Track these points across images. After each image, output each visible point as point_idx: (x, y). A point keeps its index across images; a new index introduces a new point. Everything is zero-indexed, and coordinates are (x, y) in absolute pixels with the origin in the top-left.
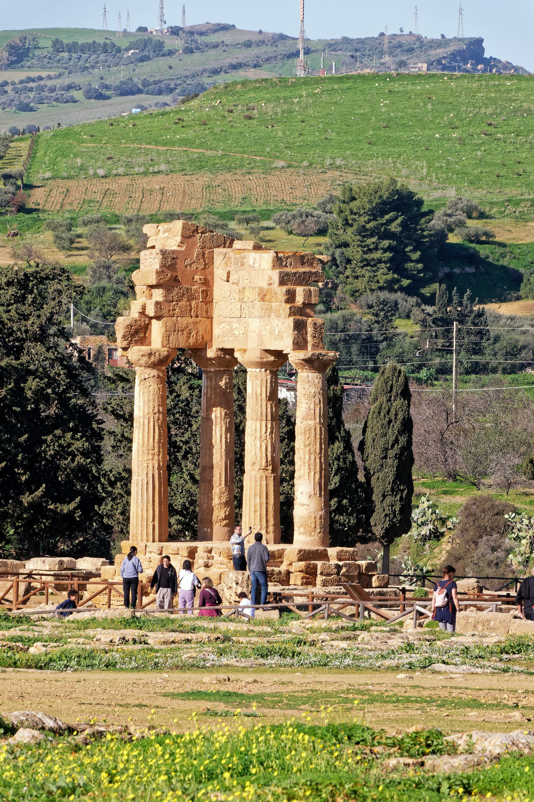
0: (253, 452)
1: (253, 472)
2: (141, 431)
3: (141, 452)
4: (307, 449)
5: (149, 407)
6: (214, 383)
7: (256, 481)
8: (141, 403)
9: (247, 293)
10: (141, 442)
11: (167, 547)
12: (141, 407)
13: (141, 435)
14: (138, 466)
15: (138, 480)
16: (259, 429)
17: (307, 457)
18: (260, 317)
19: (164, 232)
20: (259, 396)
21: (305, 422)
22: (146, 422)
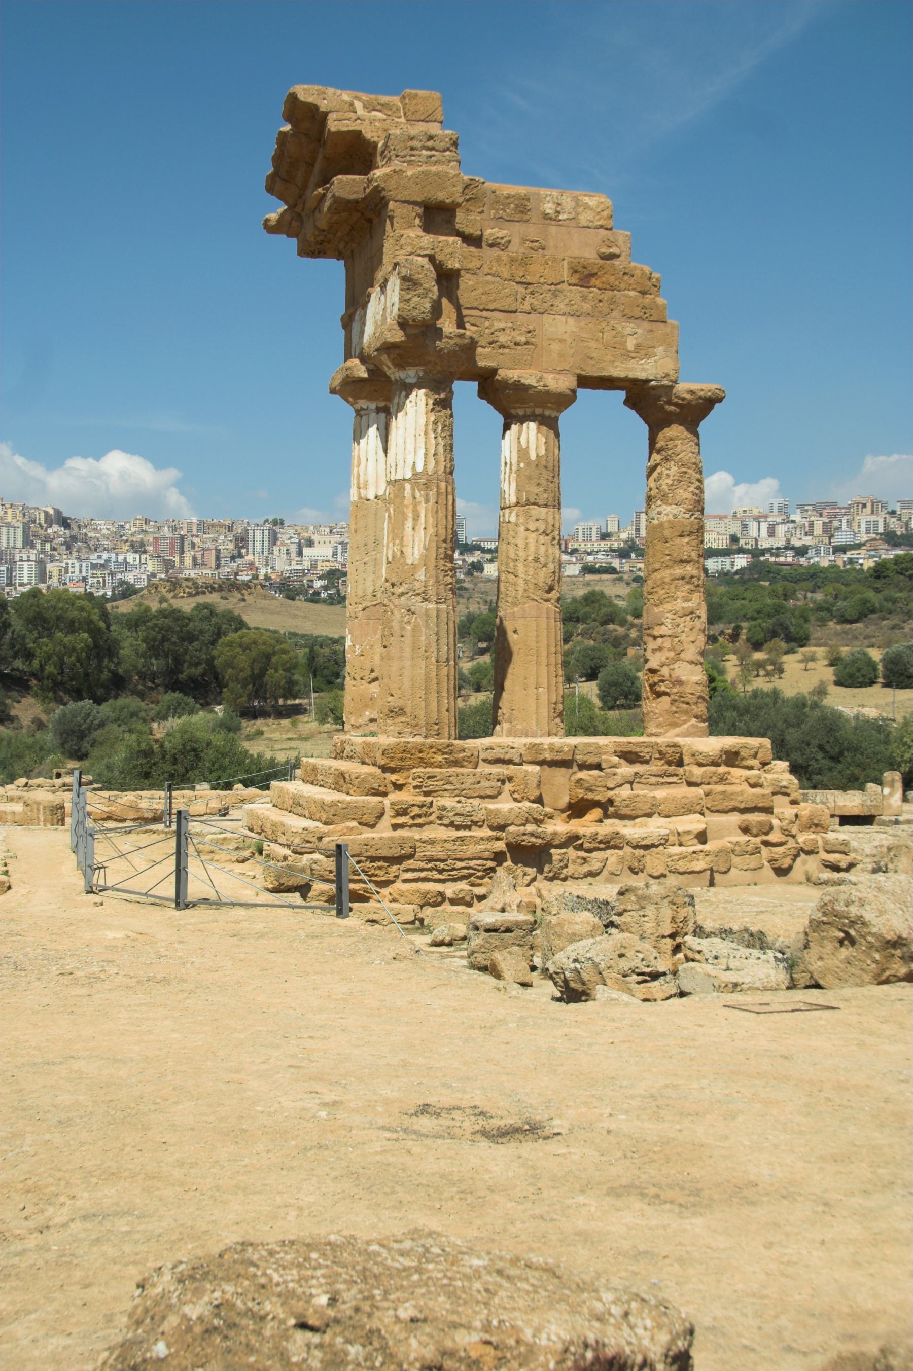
3: (442, 550)
8: (441, 449)
18: (576, 315)
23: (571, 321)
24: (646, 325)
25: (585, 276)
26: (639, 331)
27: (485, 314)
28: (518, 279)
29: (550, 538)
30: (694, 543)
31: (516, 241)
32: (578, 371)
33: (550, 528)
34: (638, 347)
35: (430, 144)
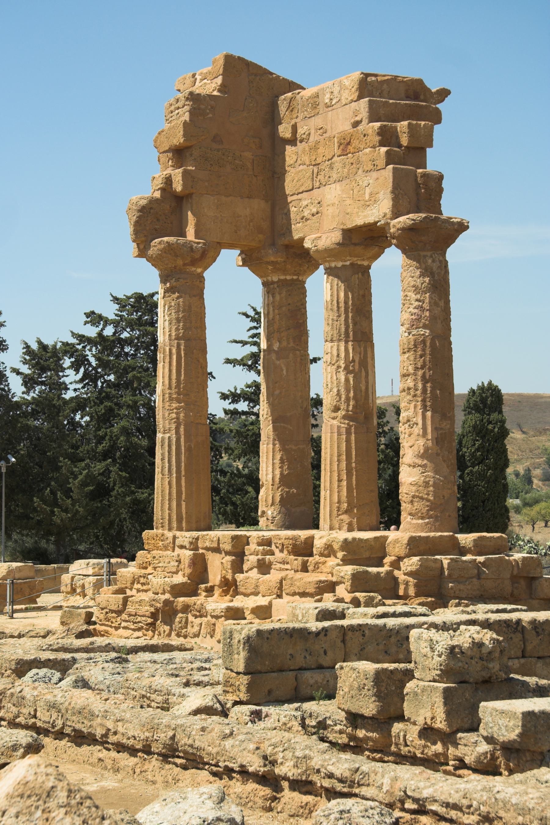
0: (335, 390)
1: (335, 422)
2: (167, 365)
4: (420, 373)
5: (177, 329)
6: (278, 297)
7: (339, 434)
8: (167, 323)
9: (321, 150)
10: (167, 382)
11: (203, 536)
12: (167, 330)
13: (167, 370)
14: (164, 418)
15: (163, 439)
16: (343, 355)
17: (420, 386)
19: (202, 80)
20: (342, 305)
21: (414, 332)
22: (174, 351)
23: (338, 185)
24: (374, 174)
25: (345, 145)
26: (371, 181)
27: (300, 196)
28: (313, 163)
29: (335, 367)
30: (412, 358)
31: (313, 132)
32: (342, 227)
33: (335, 358)
34: (371, 194)
35: (177, 106)
